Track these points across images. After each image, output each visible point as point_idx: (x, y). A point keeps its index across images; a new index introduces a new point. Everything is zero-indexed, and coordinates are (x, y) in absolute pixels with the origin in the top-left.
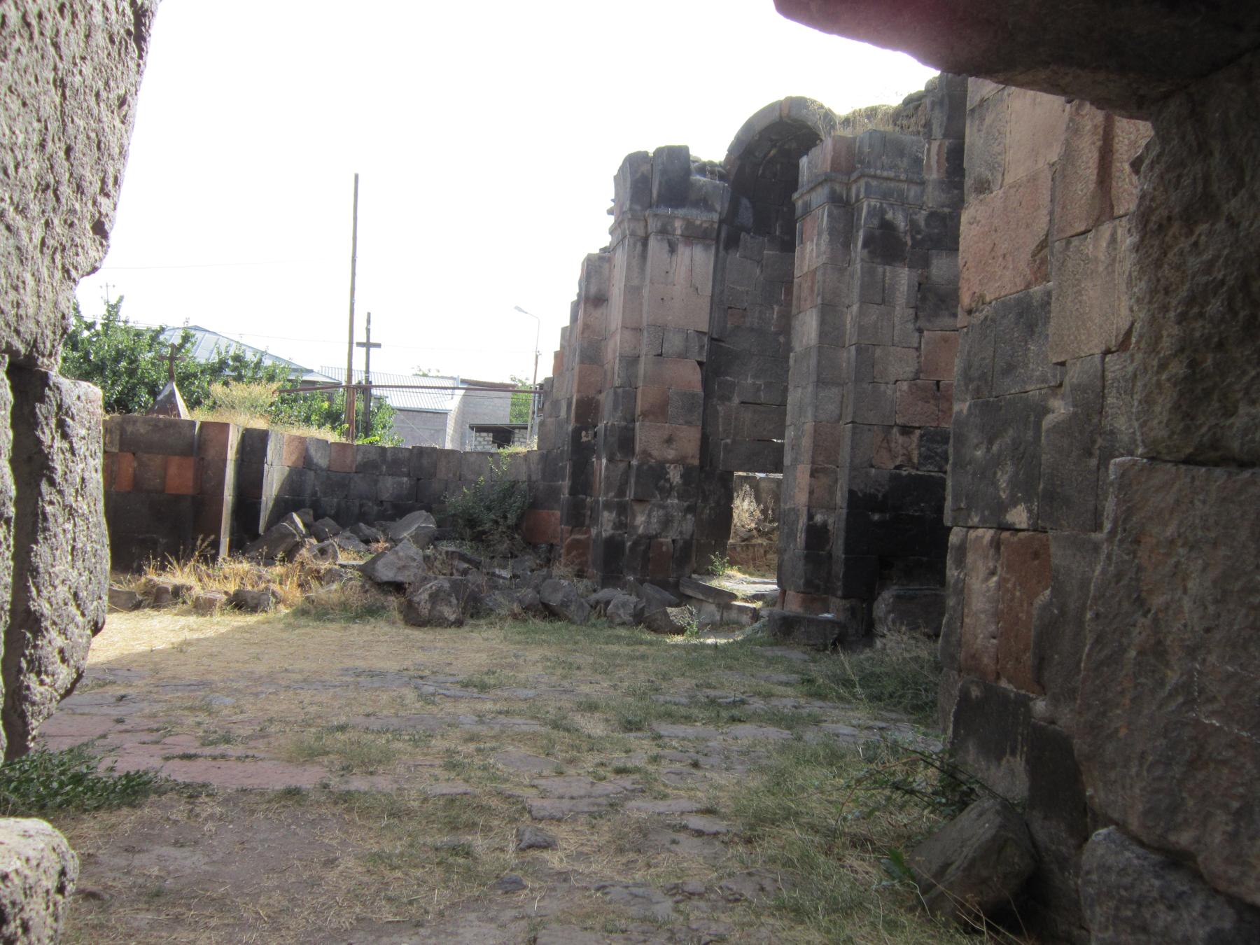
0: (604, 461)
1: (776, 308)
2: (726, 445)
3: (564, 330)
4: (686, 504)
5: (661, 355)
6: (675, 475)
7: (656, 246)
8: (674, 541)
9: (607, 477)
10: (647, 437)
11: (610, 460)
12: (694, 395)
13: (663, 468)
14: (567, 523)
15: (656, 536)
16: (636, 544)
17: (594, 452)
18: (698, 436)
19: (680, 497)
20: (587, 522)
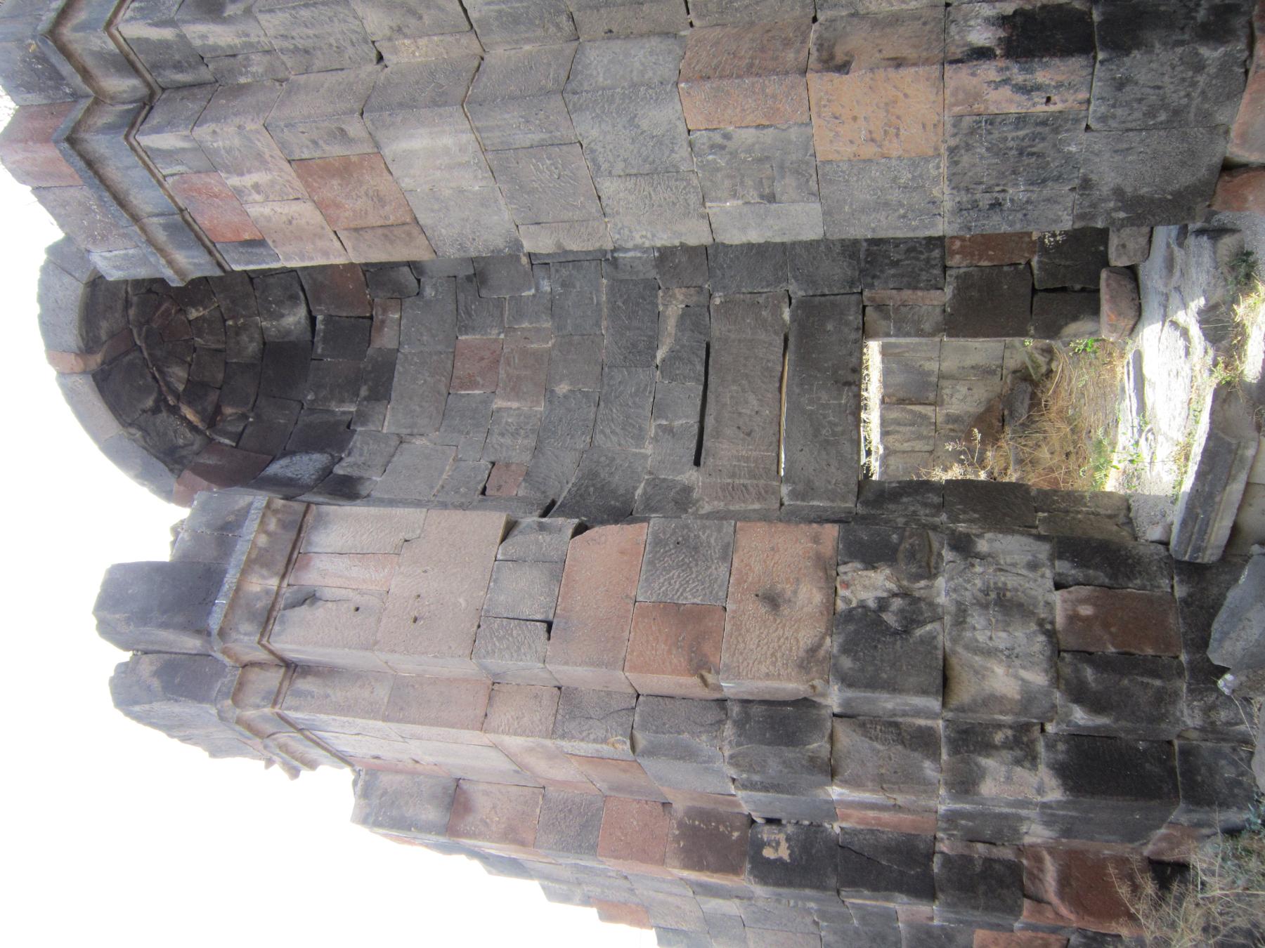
0: (836, 792)
1: (499, 403)
2: (794, 494)
3: (551, 895)
4: (948, 555)
5: (550, 625)
6: (870, 585)
7: (294, 639)
8: (1058, 586)
9: (881, 782)
10: (764, 661)
11: (832, 772)
12: (658, 542)
13: (849, 616)
14: (1015, 911)
15: (1051, 635)
16: (1079, 694)
17: (816, 828)
18: (761, 528)
19: (930, 573)
20: (1007, 853)
